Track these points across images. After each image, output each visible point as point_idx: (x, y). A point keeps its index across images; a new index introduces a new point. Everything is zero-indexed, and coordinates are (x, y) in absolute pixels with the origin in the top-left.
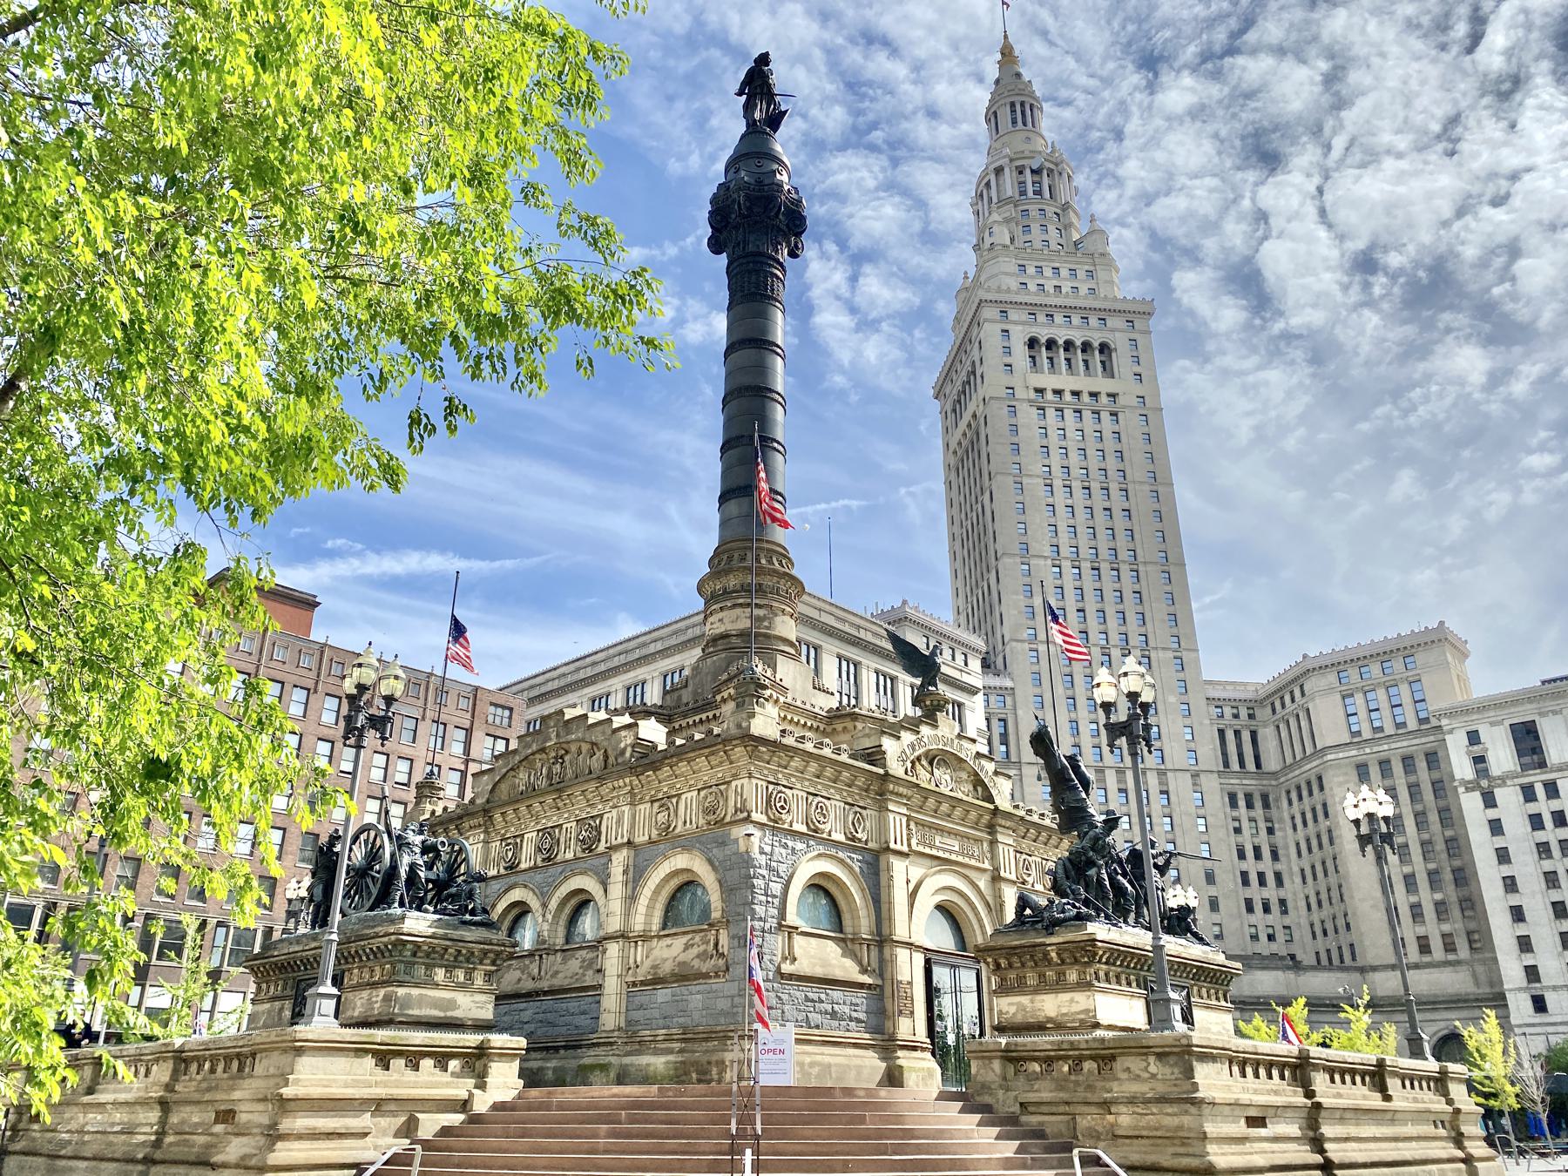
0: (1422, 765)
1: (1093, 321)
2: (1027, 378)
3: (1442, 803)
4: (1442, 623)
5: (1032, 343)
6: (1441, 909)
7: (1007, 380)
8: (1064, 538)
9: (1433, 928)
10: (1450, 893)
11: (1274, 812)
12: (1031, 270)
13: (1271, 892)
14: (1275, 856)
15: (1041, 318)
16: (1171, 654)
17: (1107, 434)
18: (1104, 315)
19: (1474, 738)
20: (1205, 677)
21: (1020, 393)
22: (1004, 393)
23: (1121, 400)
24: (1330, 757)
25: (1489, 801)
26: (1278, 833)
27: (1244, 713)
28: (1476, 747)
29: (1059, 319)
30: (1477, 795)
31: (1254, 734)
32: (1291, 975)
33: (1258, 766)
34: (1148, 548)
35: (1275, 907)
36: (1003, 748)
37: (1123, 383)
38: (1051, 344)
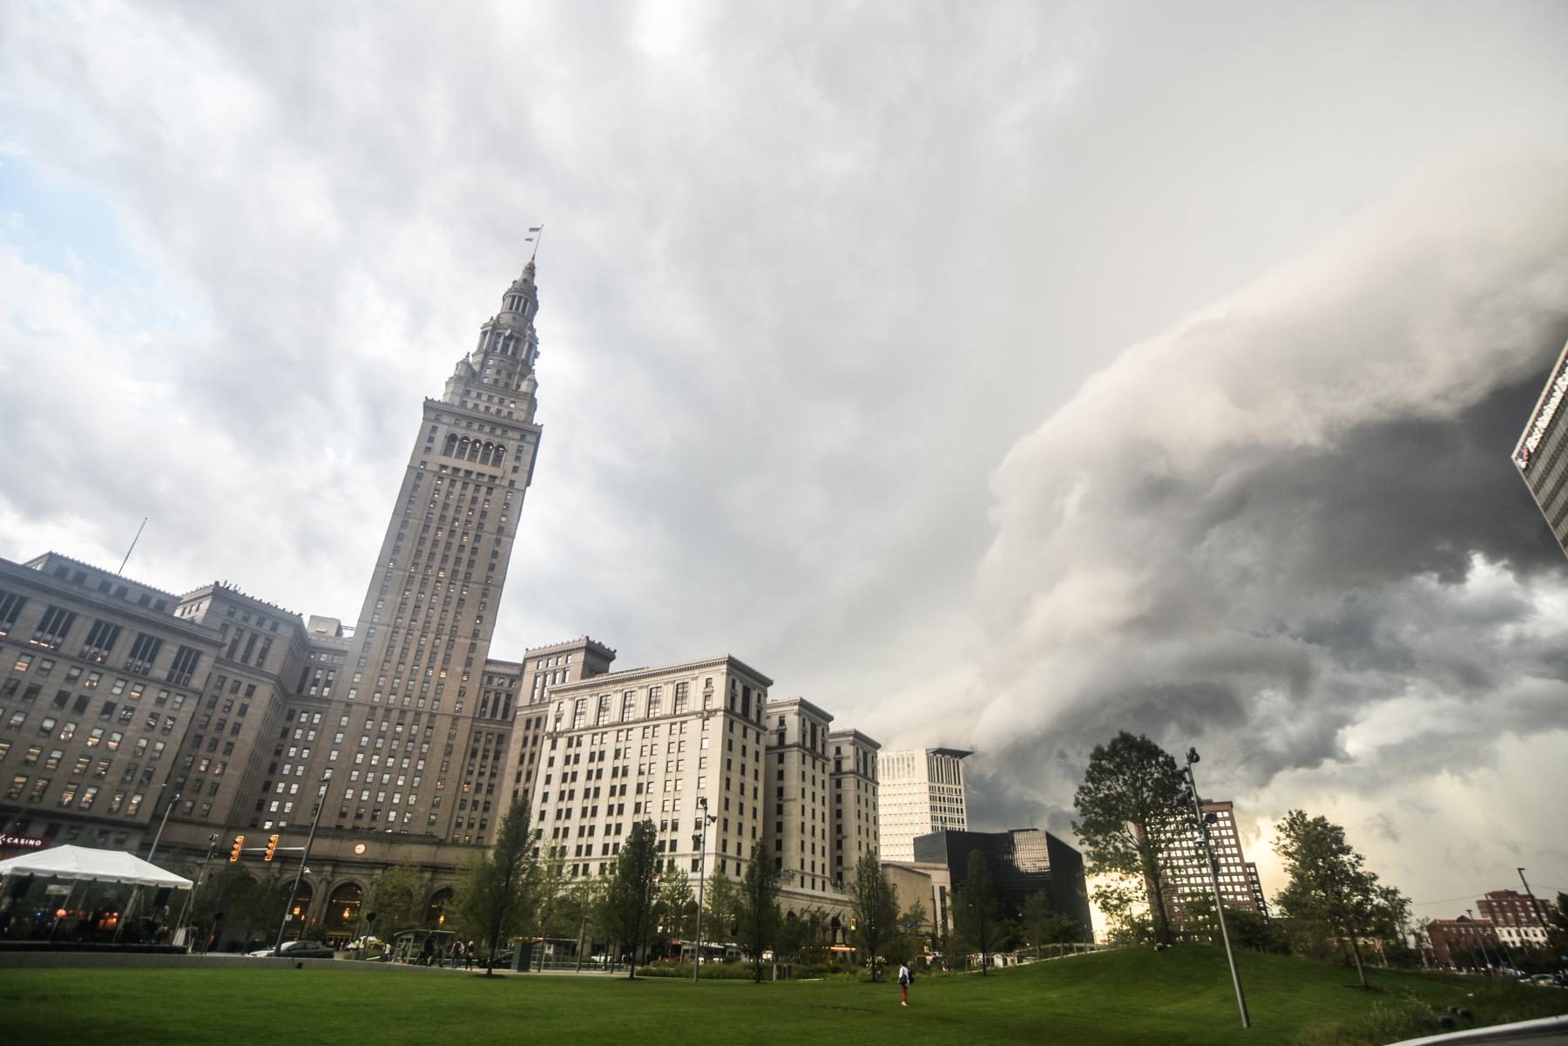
1: (499, 432)
2: (436, 458)
5: (452, 438)
7: (424, 458)
8: (424, 559)
12: (473, 394)
13: (481, 798)
14: (493, 775)
15: (464, 424)
18: (506, 428)
20: (490, 657)
22: (417, 464)
29: (476, 426)
31: (509, 697)
32: (434, 849)
33: (505, 715)
35: (480, 808)
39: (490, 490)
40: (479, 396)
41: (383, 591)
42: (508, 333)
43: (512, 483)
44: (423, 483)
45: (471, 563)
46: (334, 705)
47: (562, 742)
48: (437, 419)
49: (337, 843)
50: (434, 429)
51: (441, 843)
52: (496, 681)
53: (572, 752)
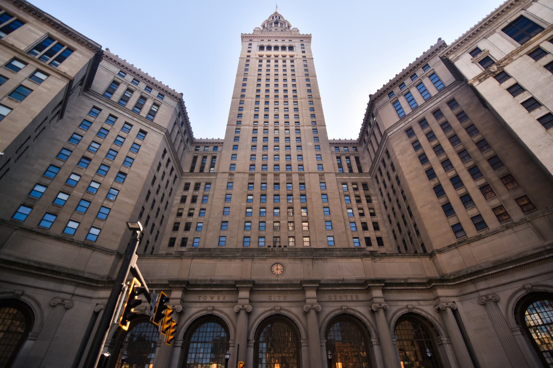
3: (467, 123)
4: (440, 39)
6: (486, 189)
9: (484, 206)
10: (491, 175)
11: (371, 191)
14: (373, 214)
16: (311, 128)
19: (475, 52)
23: (295, 57)
24: (389, 135)
26: (374, 202)
28: (479, 56)
30: (491, 81)
31: (357, 159)
32: (368, 261)
34: (302, 93)
35: (375, 243)
36: (212, 169)
39: (292, 61)
46: (219, 176)
49: (248, 262)
50: (250, 44)
51: (373, 255)
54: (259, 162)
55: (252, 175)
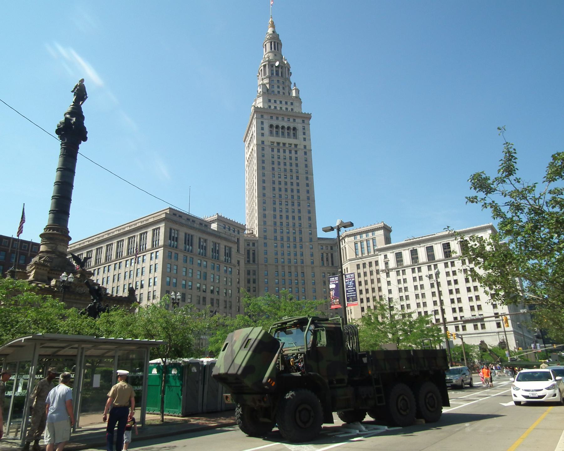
0: (374, 264)
1: (291, 120)
2: (269, 139)
5: (271, 126)
12: (272, 101)
15: (274, 118)
17: (293, 158)
19: (386, 256)
21: (265, 143)
23: (298, 147)
25: (388, 275)
27: (329, 248)
29: (280, 118)
33: (332, 264)
34: (303, 196)
37: (299, 141)
38: (277, 127)
40: (275, 102)
41: (265, 210)
42: (277, 64)
43: (305, 147)
44: (265, 152)
45: (298, 191)
47: (393, 274)
48: (262, 116)
50: (262, 123)
52: (324, 247)
53: (401, 277)
54: (279, 256)
55: (277, 266)
